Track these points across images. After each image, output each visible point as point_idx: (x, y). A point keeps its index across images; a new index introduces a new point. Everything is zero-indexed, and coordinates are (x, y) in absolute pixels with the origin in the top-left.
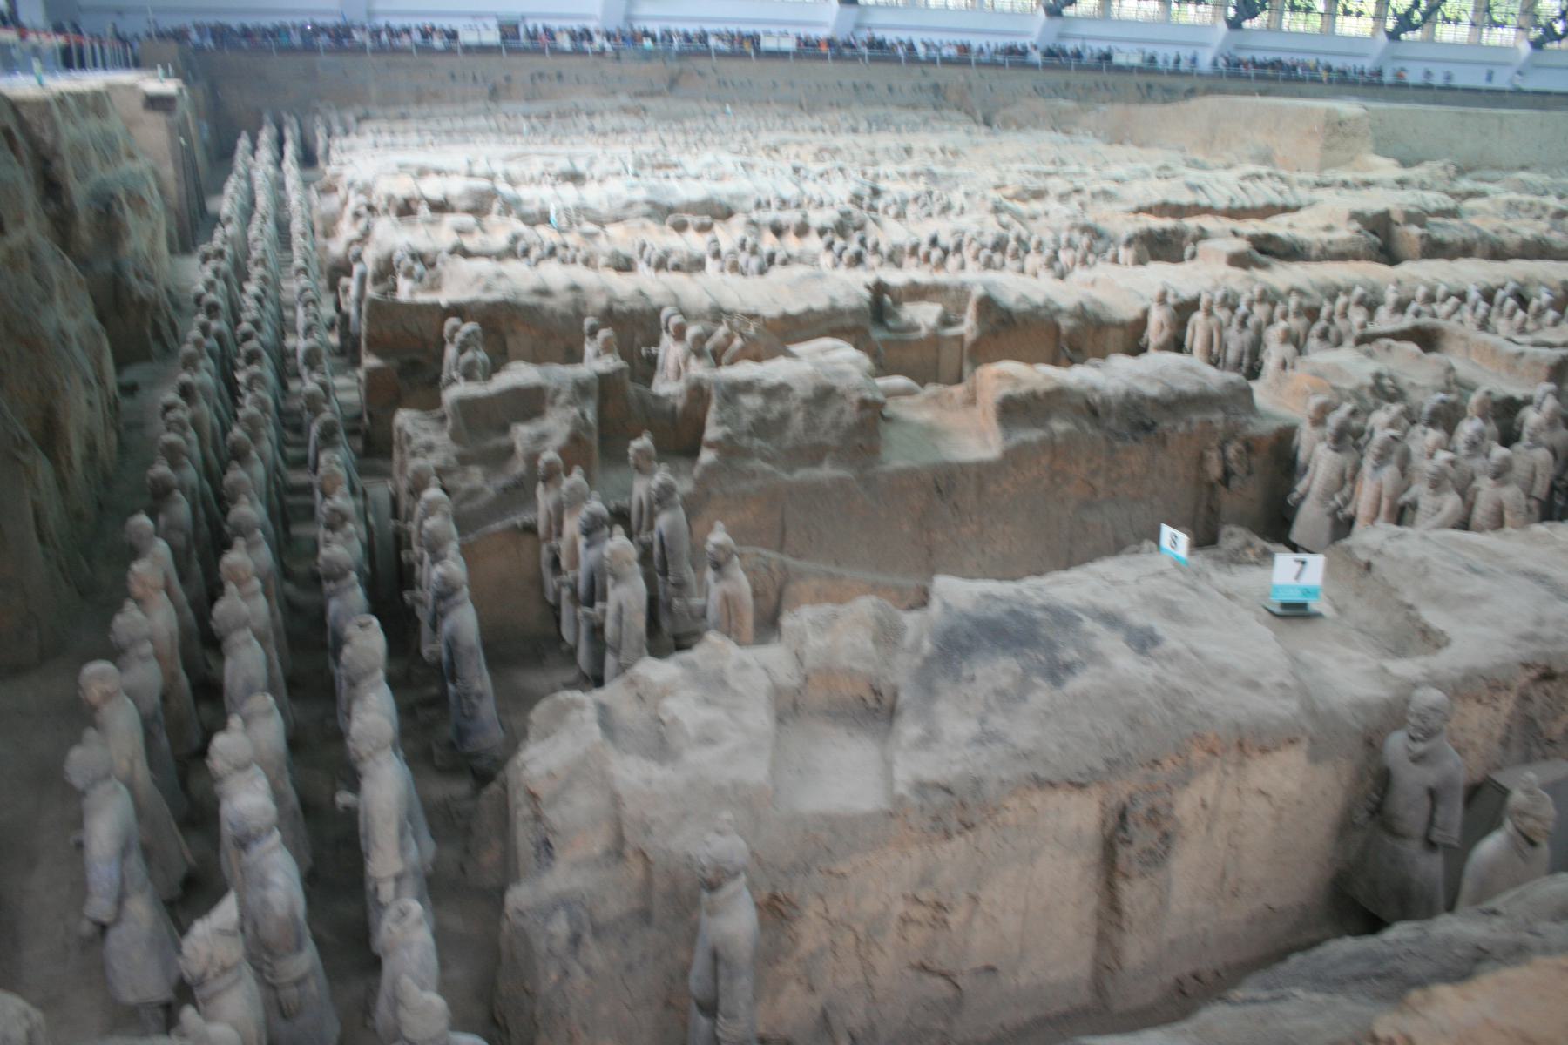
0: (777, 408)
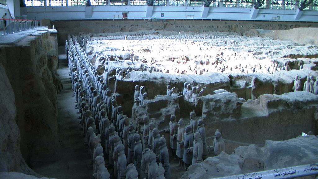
0: (218, 105)
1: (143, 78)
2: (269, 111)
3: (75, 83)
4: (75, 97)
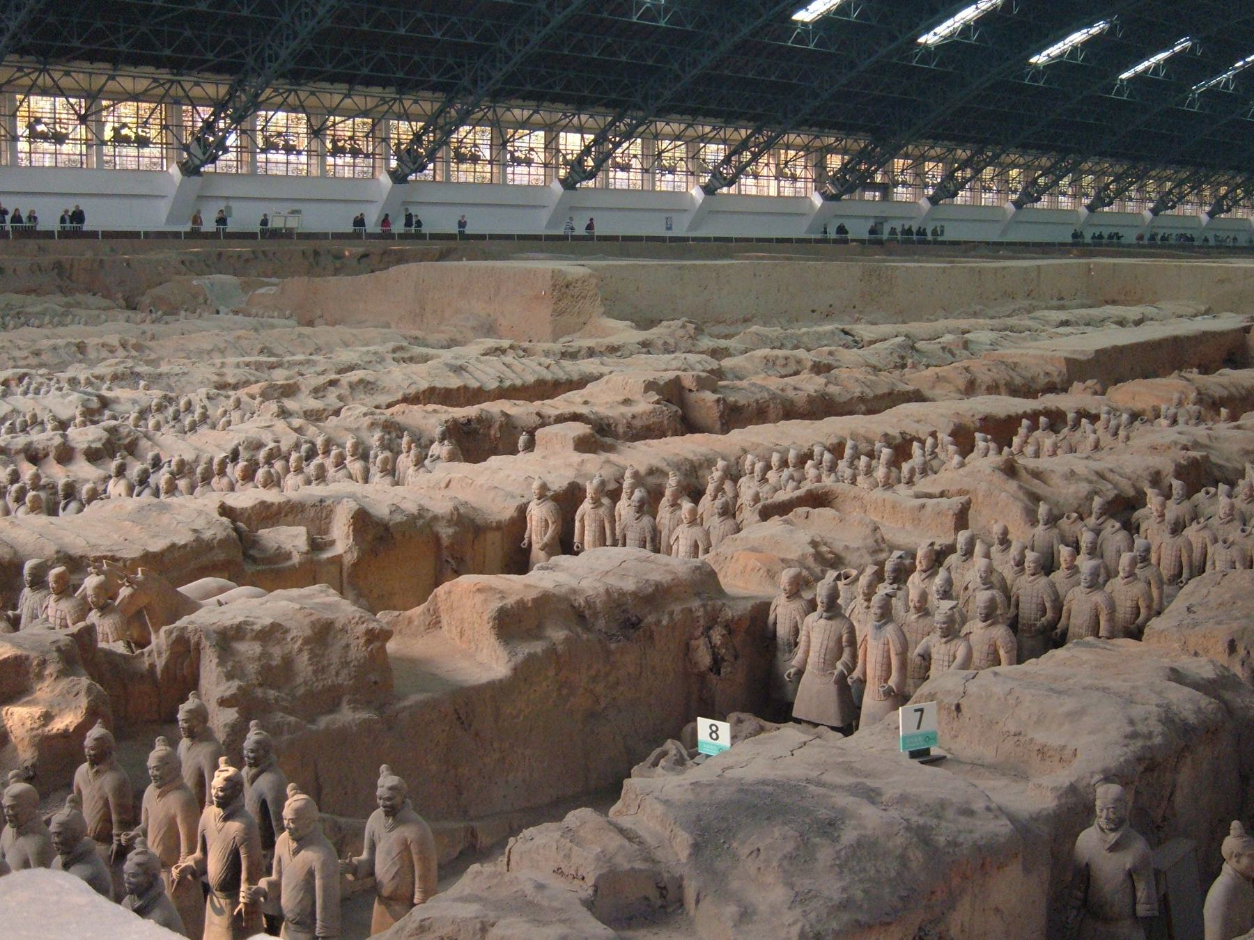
0: (277, 652)
2: (512, 654)
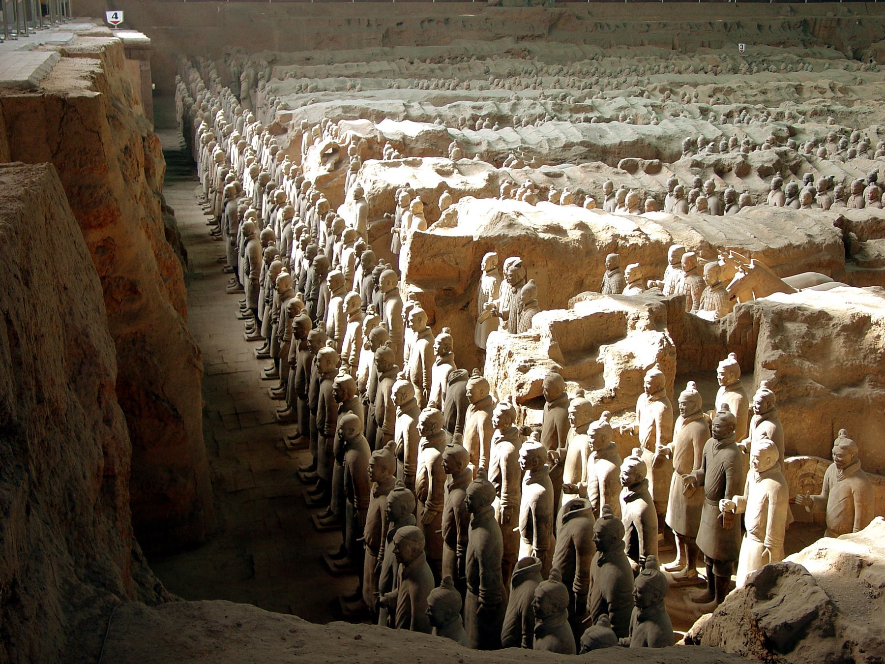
1: (511, 225)
3: (245, 244)
4: (245, 298)
